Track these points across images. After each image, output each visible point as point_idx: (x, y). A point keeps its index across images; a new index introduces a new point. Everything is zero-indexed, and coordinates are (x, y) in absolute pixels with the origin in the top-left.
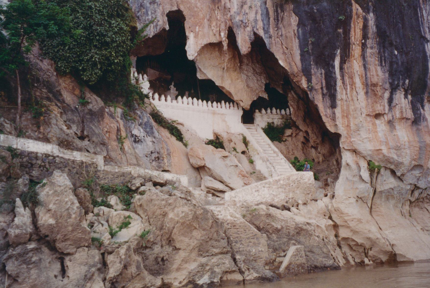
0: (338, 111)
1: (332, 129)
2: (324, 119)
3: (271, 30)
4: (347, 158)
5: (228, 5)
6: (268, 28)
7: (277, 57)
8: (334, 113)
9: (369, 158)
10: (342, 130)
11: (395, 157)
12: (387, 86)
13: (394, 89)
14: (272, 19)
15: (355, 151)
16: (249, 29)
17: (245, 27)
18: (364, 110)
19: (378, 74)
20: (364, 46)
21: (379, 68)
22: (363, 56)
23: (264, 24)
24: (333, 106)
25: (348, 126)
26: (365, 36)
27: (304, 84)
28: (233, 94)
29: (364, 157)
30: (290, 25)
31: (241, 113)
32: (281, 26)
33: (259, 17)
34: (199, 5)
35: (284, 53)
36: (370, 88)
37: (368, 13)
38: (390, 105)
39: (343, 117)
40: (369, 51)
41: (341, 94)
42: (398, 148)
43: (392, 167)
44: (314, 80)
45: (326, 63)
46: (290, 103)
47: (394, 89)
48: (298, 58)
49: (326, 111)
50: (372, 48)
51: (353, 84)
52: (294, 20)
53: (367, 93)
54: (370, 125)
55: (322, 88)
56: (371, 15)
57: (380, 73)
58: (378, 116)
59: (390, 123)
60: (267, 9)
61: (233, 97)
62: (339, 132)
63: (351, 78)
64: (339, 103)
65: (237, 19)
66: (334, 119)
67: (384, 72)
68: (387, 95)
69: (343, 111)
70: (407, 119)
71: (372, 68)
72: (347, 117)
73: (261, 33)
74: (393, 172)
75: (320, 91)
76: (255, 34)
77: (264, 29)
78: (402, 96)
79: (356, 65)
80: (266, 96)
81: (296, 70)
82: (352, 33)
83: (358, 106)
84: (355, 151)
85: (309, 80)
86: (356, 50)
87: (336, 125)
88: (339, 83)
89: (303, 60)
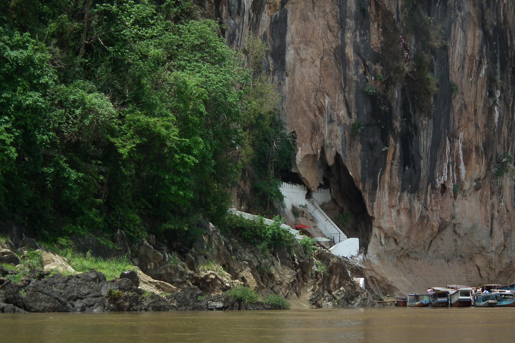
0: (375, 204)
1: (371, 215)
2: (368, 208)
3: (347, 152)
4: (375, 231)
5: (323, 132)
6: (345, 150)
7: (349, 170)
8: (373, 205)
9: (386, 232)
10: (376, 215)
11: (399, 231)
12: (400, 189)
13: (403, 191)
14: (347, 145)
15: (380, 228)
16: (334, 149)
17: (332, 148)
18: (387, 203)
19: (397, 181)
20: (392, 164)
21: (397, 178)
22: (391, 171)
23: (343, 147)
24: (373, 201)
25: (379, 213)
26: (393, 159)
27: (361, 187)
28: (310, 183)
29: (383, 231)
30: (357, 150)
31: (306, 192)
32: (352, 150)
33: (340, 142)
34: (305, 128)
35: (353, 168)
36: (392, 189)
37: (397, 143)
38: (399, 200)
39: (377, 207)
40: (394, 167)
41: (378, 194)
42: (401, 227)
43: (396, 237)
44: (366, 185)
45: (373, 175)
46: (332, 185)
47: (403, 191)
48: (360, 171)
49: (369, 204)
50: (396, 166)
51: (384, 188)
52: (359, 147)
53: (389, 193)
54: (389, 212)
55: (369, 190)
56: (398, 144)
57: (397, 181)
58: (393, 207)
59: (398, 212)
60: (345, 137)
61: (308, 184)
62: (374, 216)
63: (384, 184)
64: (376, 199)
65: (328, 142)
66: (372, 208)
67: (400, 180)
68: (399, 194)
69: (377, 204)
70: (407, 209)
71: (394, 177)
72: (379, 207)
73: (341, 153)
74: (395, 240)
75: (368, 192)
76: (336, 152)
77: (343, 151)
78: (406, 194)
79: (387, 176)
80: (323, 183)
81: (358, 179)
82: (388, 157)
83: (385, 201)
84: (380, 228)
85: (364, 186)
86: (388, 167)
87: (373, 213)
88: (378, 188)
89: (362, 173)
